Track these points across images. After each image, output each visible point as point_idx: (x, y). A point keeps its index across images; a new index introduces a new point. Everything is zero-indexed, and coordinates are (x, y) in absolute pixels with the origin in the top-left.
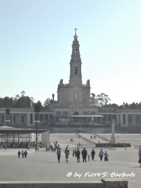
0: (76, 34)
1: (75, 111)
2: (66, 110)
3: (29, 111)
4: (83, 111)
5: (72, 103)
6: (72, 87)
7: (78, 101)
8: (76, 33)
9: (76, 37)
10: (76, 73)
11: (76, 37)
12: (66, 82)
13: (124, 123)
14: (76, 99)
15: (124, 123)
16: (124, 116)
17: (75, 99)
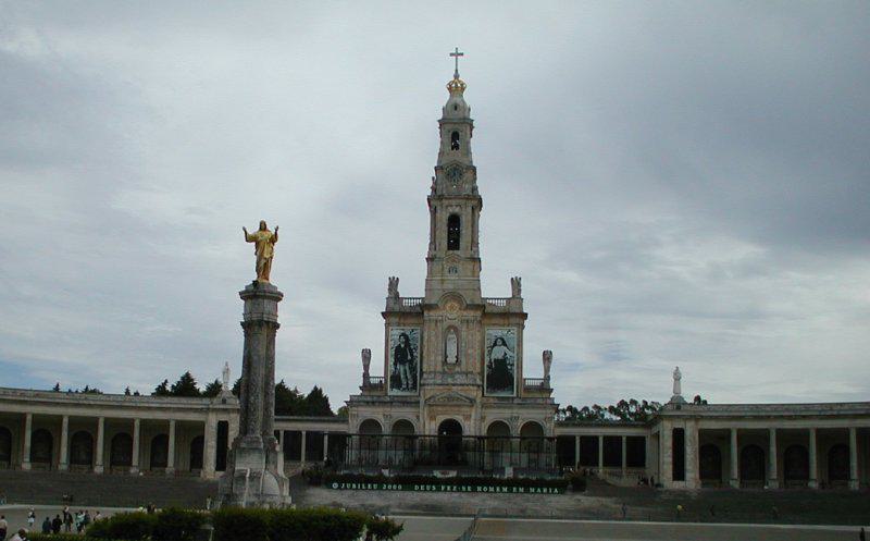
0: (456, 76)
1: (449, 417)
2: (406, 413)
3: (214, 410)
4: (483, 418)
5: (431, 381)
6: (430, 307)
7: (457, 369)
8: (457, 71)
9: (456, 88)
10: (454, 243)
11: (456, 88)
12: (414, 288)
13: (679, 474)
14: (452, 359)
15: (679, 474)
16: (679, 435)
17: (445, 362)
